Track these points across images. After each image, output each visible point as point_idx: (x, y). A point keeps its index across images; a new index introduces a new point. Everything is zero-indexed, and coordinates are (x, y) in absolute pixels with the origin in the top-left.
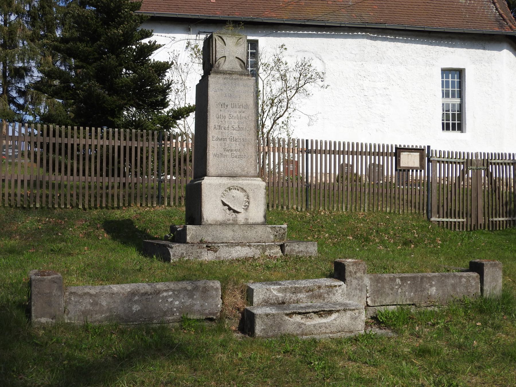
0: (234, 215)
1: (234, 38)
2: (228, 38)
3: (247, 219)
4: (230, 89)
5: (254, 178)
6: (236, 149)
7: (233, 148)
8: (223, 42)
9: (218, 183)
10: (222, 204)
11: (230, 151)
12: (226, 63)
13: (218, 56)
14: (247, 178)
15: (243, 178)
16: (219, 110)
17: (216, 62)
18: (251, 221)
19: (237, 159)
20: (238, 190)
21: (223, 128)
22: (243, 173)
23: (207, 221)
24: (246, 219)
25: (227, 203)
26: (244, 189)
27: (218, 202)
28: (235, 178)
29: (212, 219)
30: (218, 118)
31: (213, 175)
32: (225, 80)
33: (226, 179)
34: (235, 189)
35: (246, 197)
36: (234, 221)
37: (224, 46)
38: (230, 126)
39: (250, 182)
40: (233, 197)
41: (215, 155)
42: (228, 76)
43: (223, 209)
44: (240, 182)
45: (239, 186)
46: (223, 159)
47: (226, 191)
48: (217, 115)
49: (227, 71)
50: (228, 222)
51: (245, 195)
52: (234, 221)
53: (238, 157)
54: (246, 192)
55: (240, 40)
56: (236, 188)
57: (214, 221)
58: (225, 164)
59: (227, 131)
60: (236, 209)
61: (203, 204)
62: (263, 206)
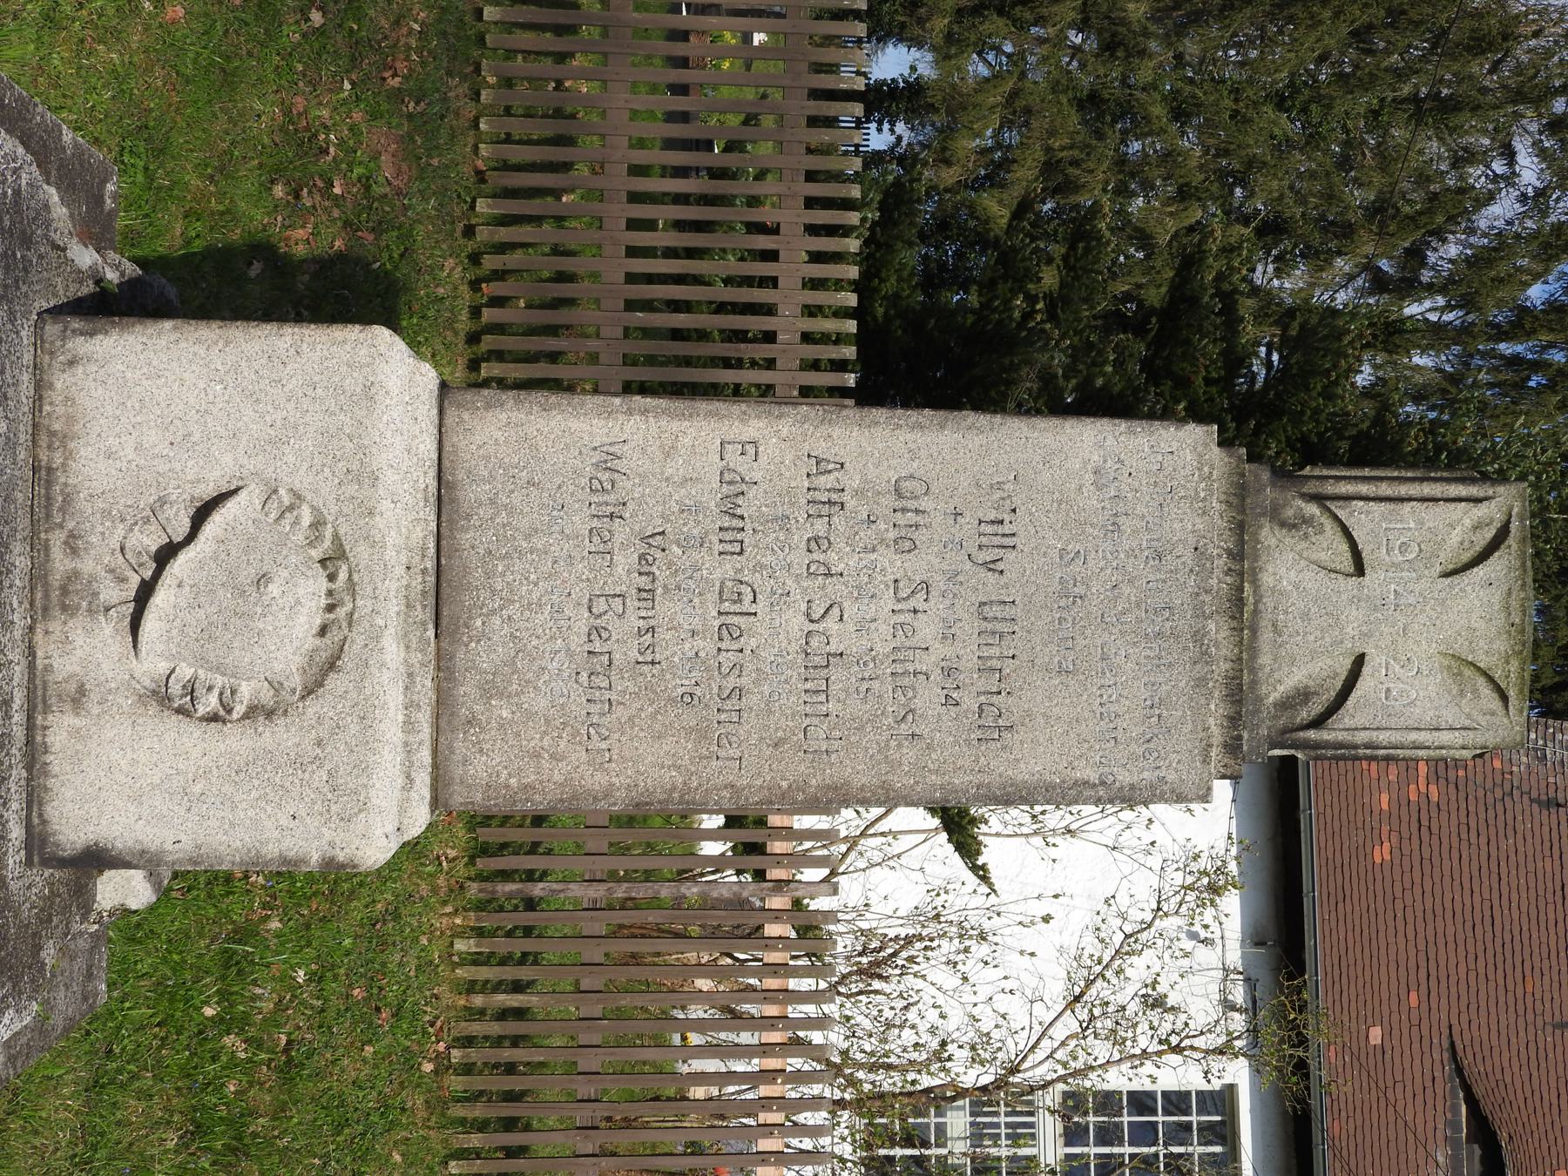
0: (118, 594)
1: (1502, 645)
2: (1496, 597)
3: (78, 698)
4: (1126, 590)
5: (423, 779)
6: (662, 634)
7: (666, 608)
8: (1466, 557)
9: (381, 460)
10: (207, 491)
11: (643, 581)
12: (1313, 580)
13: (1365, 520)
14: (424, 718)
15: (425, 685)
16: (956, 501)
17: (1319, 499)
18: (60, 730)
19: (577, 641)
20: (323, 631)
21: (820, 527)
22: (467, 690)
23: (72, 363)
24: (82, 691)
25: (214, 526)
26: (332, 681)
27: (228, 459)
28: (424, 614)
29: (82, 399)
30: (899, 493)
31: (453, 439)
32: (1189, 557)
33: (418, 533)
34: (330, 608)
35: (267, 697)
36: (65, 591)
37: (1439, 569)
38: (836, 588)
39: (390, 728)
40: (262, 579)
41: (609, 462)
42: (1219, 582)
43: (162, 501)
44: (392, 651)
45: (357, 640)
46: (580, 522)
47: (317, 524)
48: (920, 488)
49: (1255, 582)
50: (57, 539)
51: (277, 687)
52: (65, 591)
53: (597, 646)
54: (309, 692)
55: (1486, 691)
56: (341, 612)
57: (71, 420)
58: (539, 542)
59: (799, 559)
60: (161, 598)
61: (209, 332)
62: (187, 844)
